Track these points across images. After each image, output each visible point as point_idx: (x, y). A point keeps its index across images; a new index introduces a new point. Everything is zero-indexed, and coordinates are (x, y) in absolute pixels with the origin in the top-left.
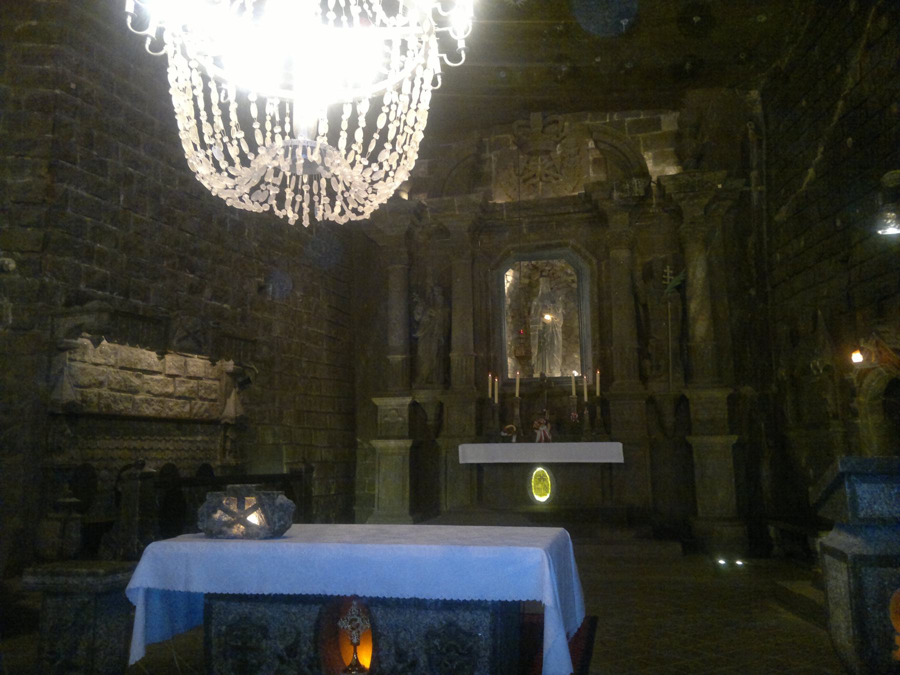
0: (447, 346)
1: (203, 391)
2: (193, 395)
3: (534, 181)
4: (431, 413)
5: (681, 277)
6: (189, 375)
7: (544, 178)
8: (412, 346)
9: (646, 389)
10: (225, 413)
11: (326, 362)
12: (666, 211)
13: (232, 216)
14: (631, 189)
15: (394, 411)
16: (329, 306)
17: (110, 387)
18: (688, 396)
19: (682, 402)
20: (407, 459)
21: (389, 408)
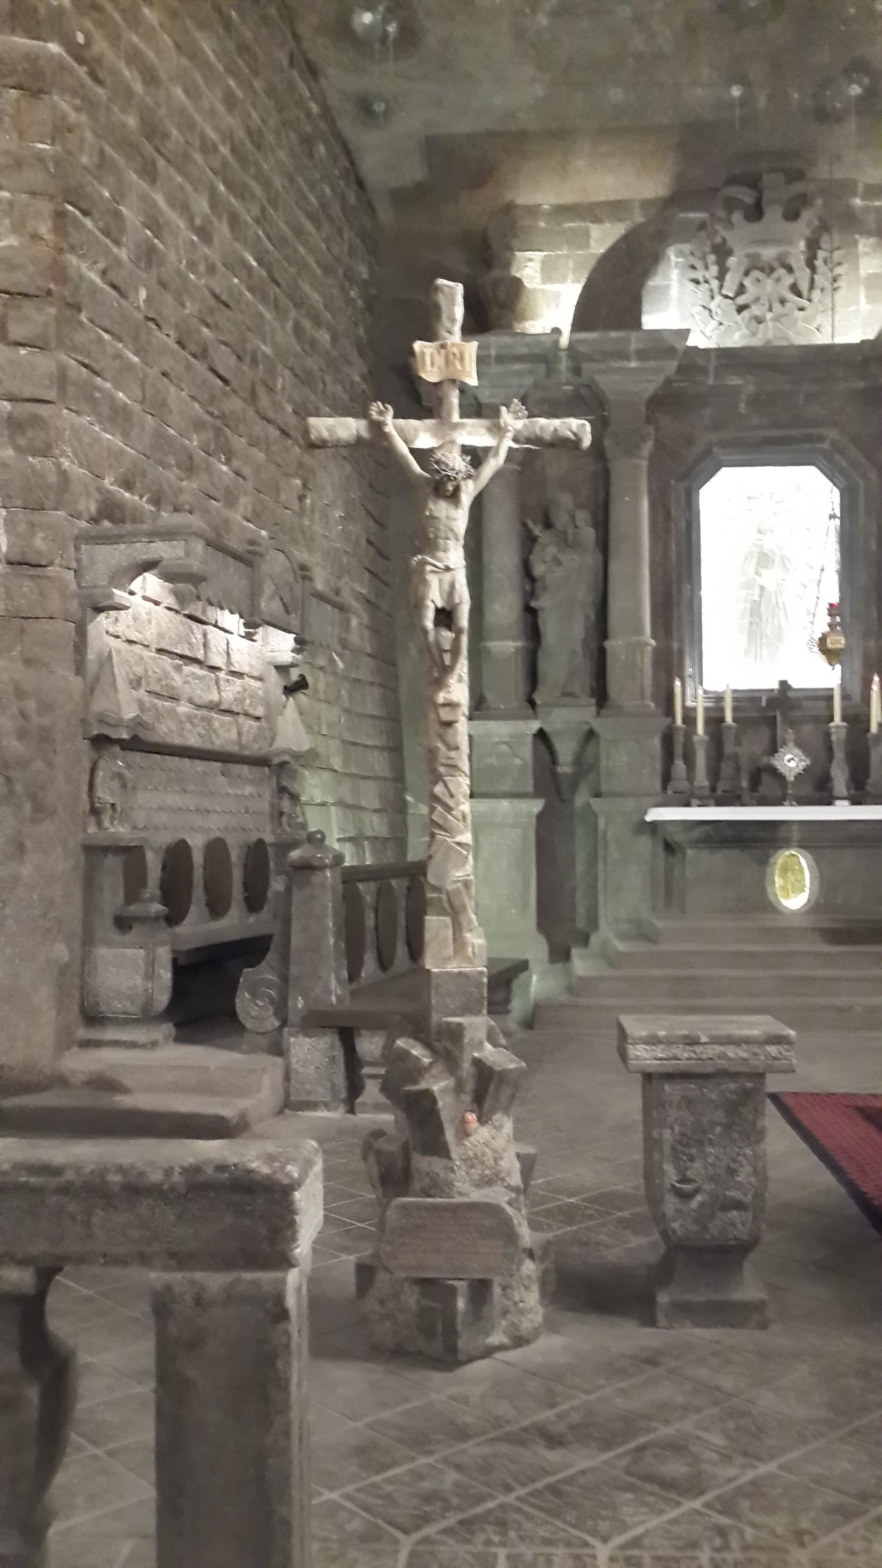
3: (756, 310)
6: (234, 669)
7: (777, 306)
10: (281, 743)
11: (369, 650)
15: (504, 748)
17: (148, 689)
21: (496, 740)
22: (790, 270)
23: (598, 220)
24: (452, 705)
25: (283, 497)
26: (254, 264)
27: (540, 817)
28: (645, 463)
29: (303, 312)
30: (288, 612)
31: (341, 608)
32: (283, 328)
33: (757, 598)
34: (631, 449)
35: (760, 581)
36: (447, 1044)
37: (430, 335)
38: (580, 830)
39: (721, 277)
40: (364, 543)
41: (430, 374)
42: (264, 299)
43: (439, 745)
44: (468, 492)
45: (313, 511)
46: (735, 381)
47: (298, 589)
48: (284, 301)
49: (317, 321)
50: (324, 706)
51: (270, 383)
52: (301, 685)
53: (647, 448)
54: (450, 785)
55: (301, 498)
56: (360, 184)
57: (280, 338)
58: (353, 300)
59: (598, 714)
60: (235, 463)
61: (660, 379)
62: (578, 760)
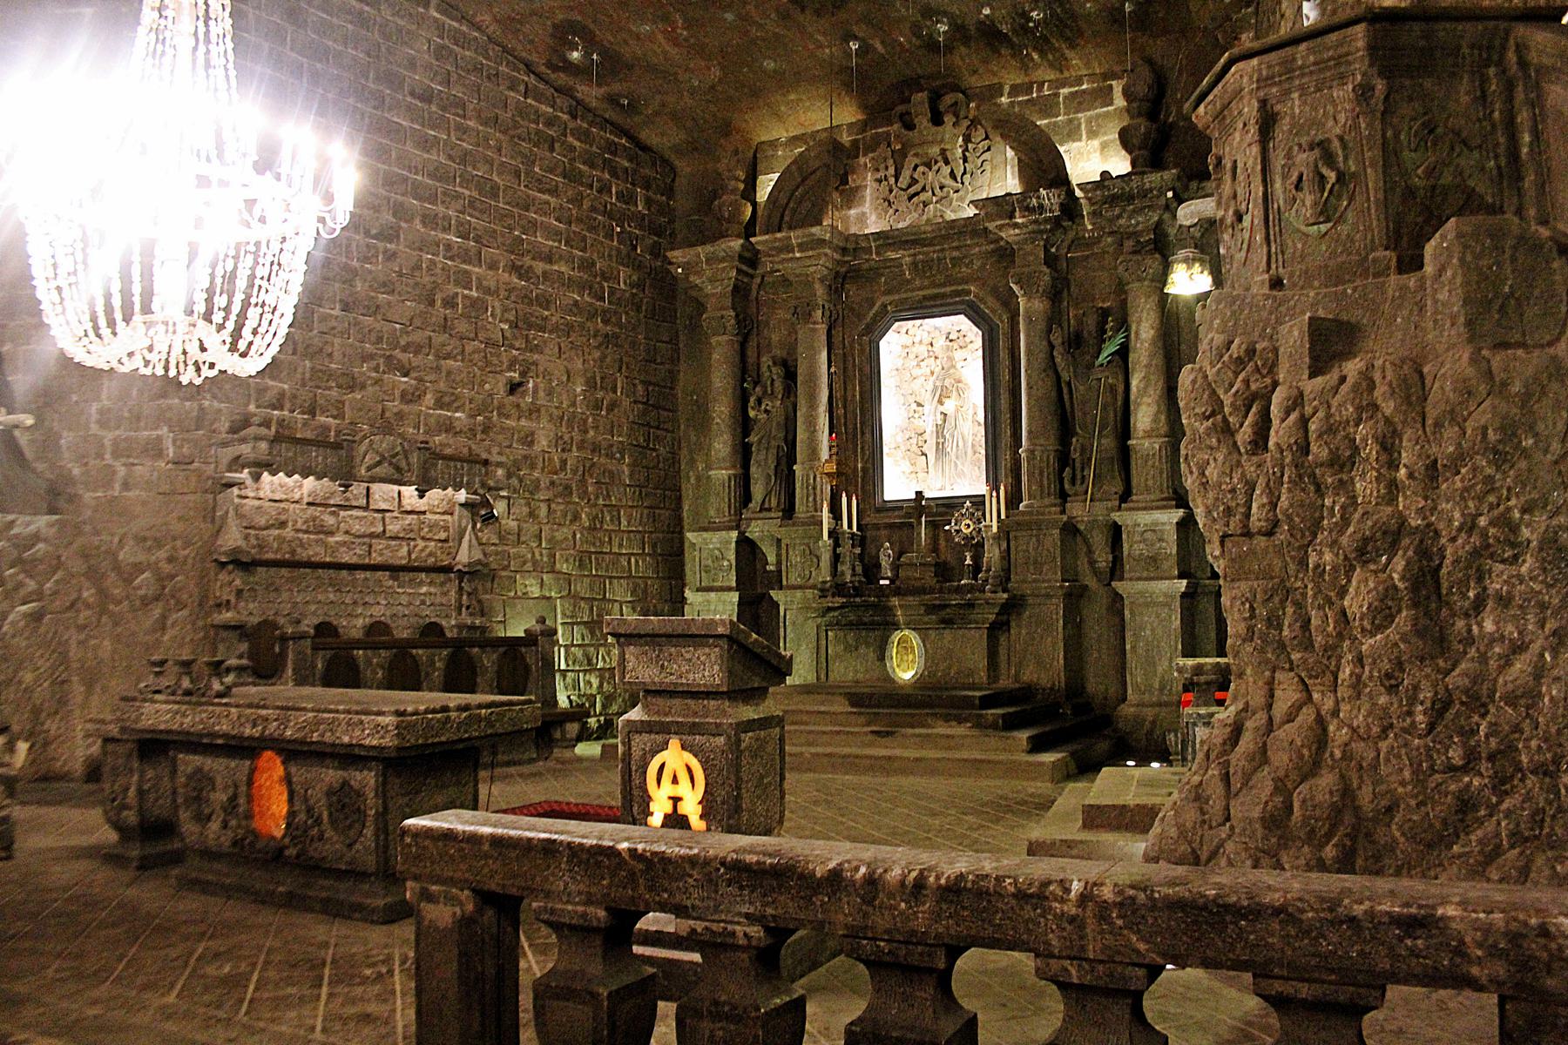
1: (426, 530)
2: (411, 535)
3: (923, 197)
9: (1063, 512)
13: (466, 292)
14: (1041, 206)
18: (1117, 519)
19: (1116, 531)
22: (947, 162)
33: (940, 422)
35: (941, 408)
46: (893, 255)
60: (414, 375)
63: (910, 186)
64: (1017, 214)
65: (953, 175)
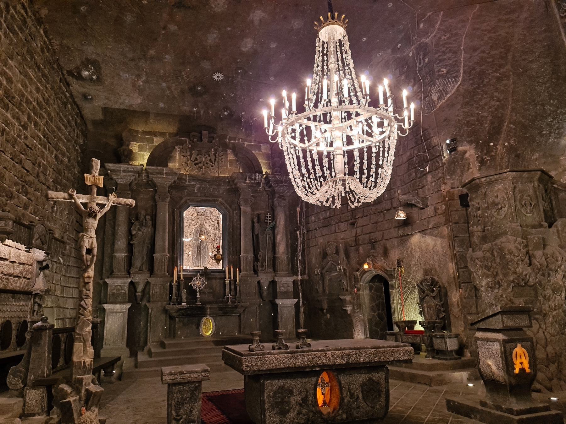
0: (152, 250)
3: (200, 165)
4: (140, 288)
5: (273, 223)
7: (206, 165)
8: (130, 248)
12: (266, 191)
14: (255, 179)
15: (119, 287)
16: (76, 221)
19: (273, 283)
20: (126, 315)
22: (209, 156)
23: (156, 136)
24: (89, 277)
25: (46, 206)
26: (42, 137)
27: (129, 309)
28: (168, 203)
29: (59, 152)
30: (43, 244)
31: (63, 242)
32: (51, 157)
34: (164, 200)
36: (77, 385)
37: (89, 172)
38: (143, 313)
39: (191, 155)
40: (75, 221)
41: (88, 183)
42: (45, 148)
43: (83, 289)
44: (99, 216)
45: (56, 212)
47: (47, 237)
48: (51, 148)
49: (63, 155)
50: (55, 274)
51: (45, 173)
52: (47, 267)
53: (168, 199)
54: (86, 302)
55: (53, 208)
56: (82, 117)
57: (49, 159)
58: (77, 150)
59: (150, 277)
61: (173, 181)
62: (143, 291)
63: (195, 161)
64: (247, 180)
65: (210, 160)
